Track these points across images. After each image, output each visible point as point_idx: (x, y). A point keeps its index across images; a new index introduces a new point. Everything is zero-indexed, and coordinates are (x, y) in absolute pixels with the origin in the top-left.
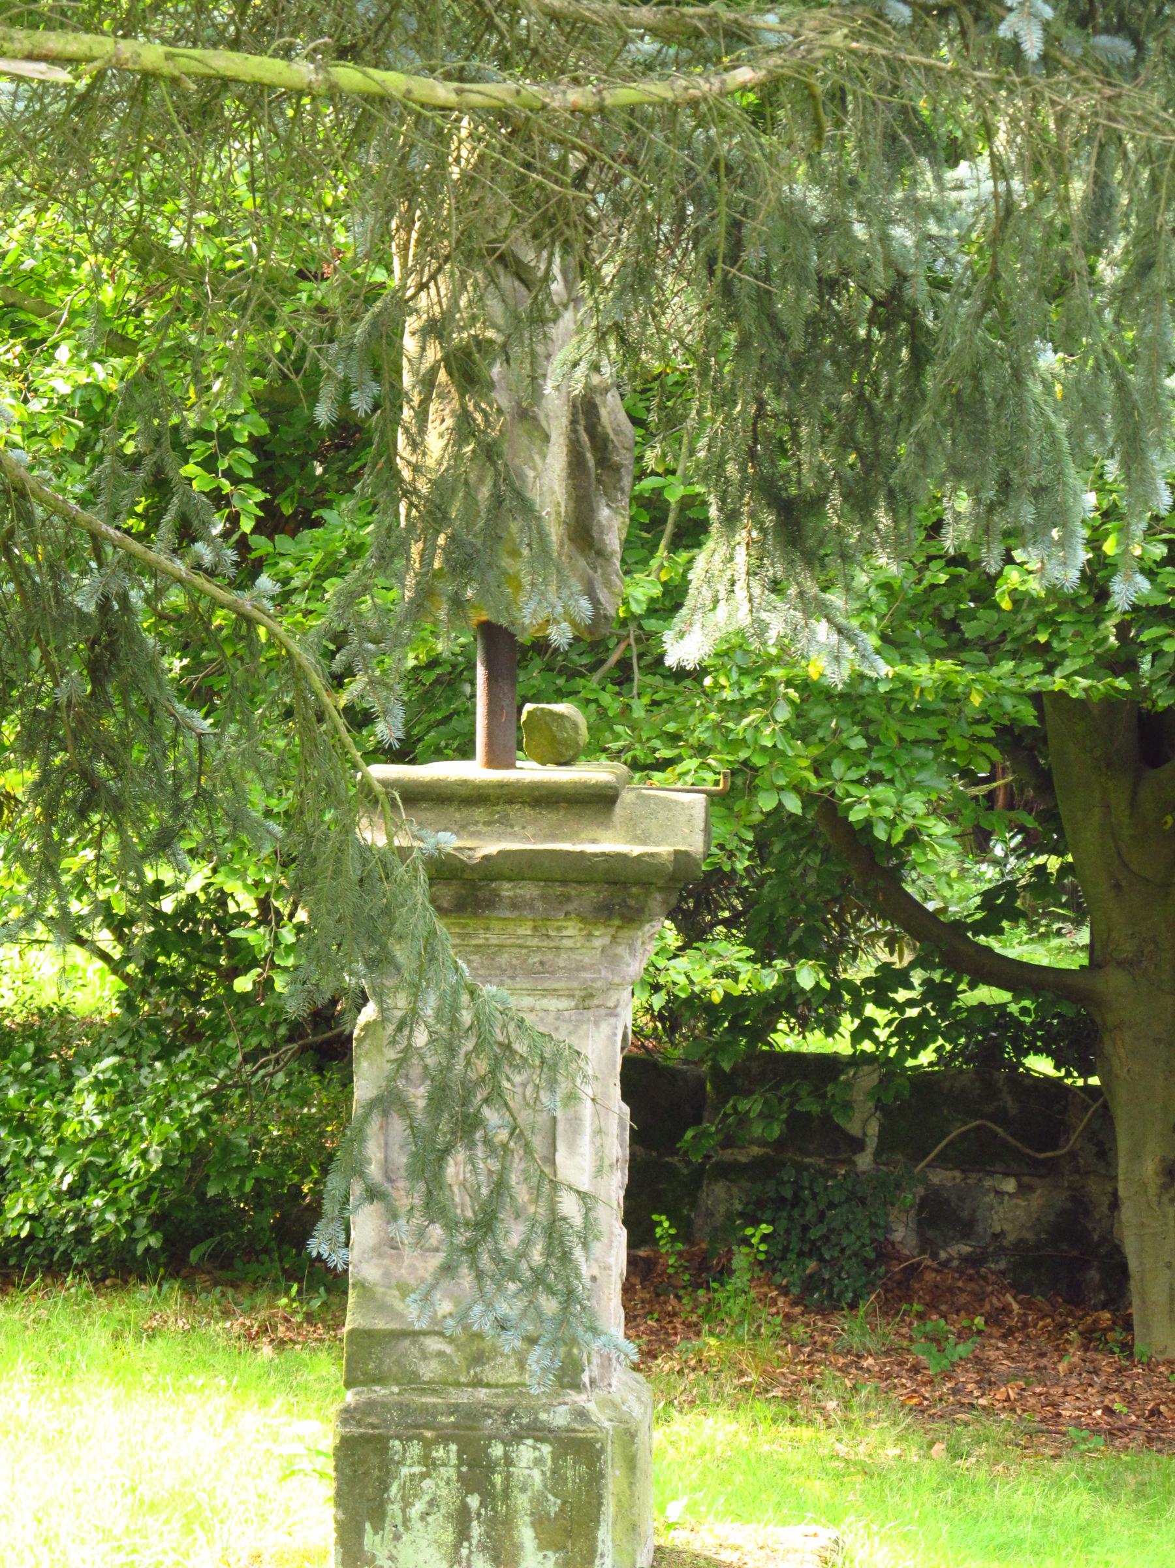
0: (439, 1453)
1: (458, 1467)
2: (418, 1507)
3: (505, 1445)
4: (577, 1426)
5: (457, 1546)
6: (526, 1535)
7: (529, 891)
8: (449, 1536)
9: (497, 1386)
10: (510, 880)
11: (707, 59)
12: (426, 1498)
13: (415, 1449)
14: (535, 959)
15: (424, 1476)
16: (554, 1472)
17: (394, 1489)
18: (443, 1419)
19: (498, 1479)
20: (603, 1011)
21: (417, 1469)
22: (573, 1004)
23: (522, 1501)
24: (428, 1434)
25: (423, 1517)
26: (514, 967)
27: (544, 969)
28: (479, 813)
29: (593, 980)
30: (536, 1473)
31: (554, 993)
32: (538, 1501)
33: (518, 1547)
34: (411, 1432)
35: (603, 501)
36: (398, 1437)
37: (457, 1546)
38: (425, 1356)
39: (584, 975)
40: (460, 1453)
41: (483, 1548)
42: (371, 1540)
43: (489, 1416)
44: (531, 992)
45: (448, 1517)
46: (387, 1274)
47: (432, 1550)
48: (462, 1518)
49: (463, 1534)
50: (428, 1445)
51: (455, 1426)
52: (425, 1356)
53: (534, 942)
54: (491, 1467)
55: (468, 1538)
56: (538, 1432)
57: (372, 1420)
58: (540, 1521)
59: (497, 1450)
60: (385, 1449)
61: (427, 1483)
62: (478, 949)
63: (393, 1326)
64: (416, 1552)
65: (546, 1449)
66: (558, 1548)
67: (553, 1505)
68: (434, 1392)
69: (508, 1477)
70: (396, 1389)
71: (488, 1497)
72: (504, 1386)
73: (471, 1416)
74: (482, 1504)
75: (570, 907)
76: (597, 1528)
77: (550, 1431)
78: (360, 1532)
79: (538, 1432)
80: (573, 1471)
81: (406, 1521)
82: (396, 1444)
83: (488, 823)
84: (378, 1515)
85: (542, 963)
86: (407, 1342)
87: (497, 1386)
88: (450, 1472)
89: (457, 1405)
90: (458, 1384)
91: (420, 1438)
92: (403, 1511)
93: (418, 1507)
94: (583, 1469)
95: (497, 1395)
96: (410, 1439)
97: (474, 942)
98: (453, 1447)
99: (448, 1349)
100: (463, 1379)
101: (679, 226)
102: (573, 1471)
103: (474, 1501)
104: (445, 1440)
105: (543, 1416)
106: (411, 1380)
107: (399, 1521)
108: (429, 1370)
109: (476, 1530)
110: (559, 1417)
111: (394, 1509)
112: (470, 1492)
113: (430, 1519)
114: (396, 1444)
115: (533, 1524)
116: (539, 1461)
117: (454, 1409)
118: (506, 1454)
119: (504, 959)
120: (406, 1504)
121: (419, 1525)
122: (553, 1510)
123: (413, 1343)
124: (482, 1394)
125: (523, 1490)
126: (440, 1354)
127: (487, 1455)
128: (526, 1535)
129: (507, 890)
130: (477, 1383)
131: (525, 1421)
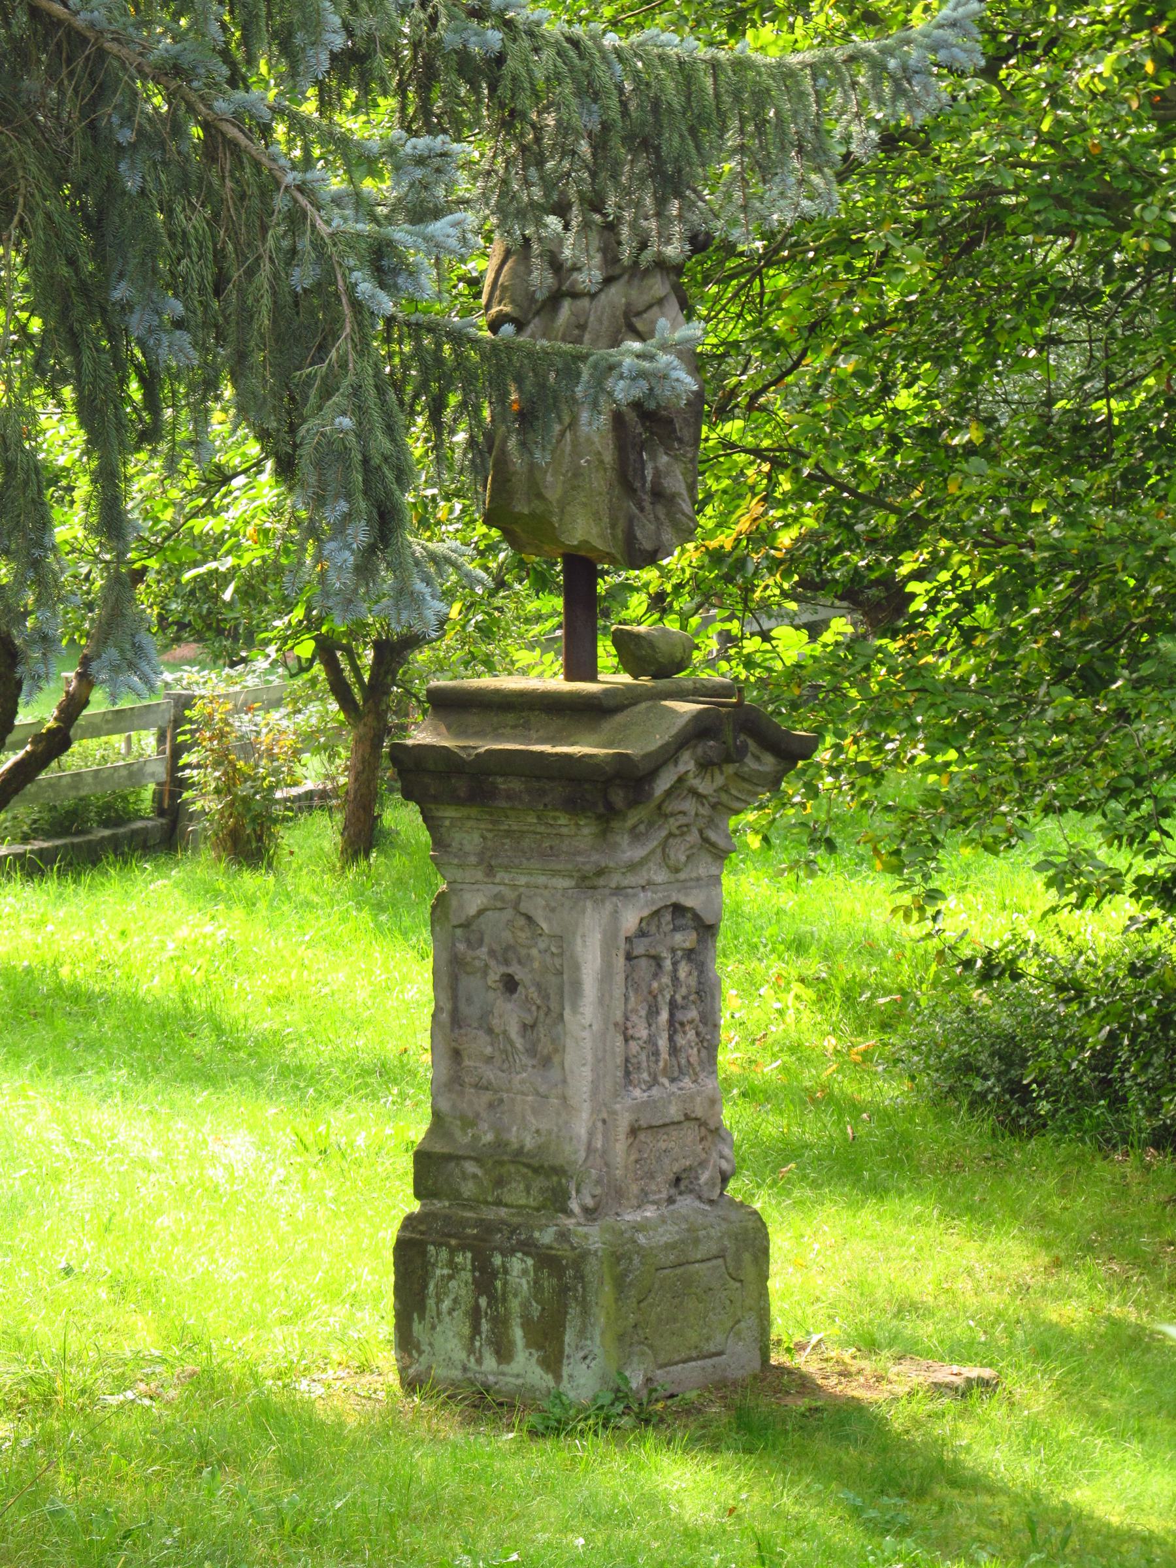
0: (459, 1259)
1: (473, 1270)
2: (446, 1304)
3: (504, 1255)
4: (555, 1245)
5: (472, 1339)
6: (518, 1334)
7: (516, 785)
8: (466, 1331)
9: (512, 1206)
10: (502, 775)
11: (237, 145)
12: (452, 1296)
13: (444, 1254)
14: (546, 844)
15: (451, 1277)
16: (535, 1283)
17: (431, 1287)
18: (469, 1231)
19: (499, 1284)
20: (607, 891)
21: (446, 1272)
22: (573, 883)
23: (515, 1305)
24: (453, 1242)
25: (451, 1311)
26: (532, 850)
27: (552, 853)
28: (510, 718)
29: (584, 864)
30: (524, 1281)
31: (555, 873)
32: (525, 1305)
33: (512, 1343)
34: (442, 1240)
35: (661, 450)
36: (433, 1243)
37: (472, 1339)
38: (464, 1177)
39: (580, 859)
40: (473, 1260)
41: (490, 1343)
42: (417, 1328)
43: (500, 1231)
44: (544, 871)
45: (466, 1313)
46: (454, 1106)
47: (456, 1341)
48: (475, 1315)
49: (476, 1330)
50: (453, 1251)
51: (475, 1237)
52: (464, 1177)
53: (541, 829)
54: (494, 1275)
55: (479, 1333)
56: (528, 1247)
57: (422, 1228)
58: (527, 1324)
59: (497, 1260)
60: (424, 1253)
61: (453, 1284)
62: (509, 833)
63: (446, 1150)
64: (446, 1341)
65: (530, 1262)
66: (540, 1347)
67: (536, 1310)
68: (472, 1208)
69: (505, 1284)
70: (447, 1204)
71: (492, 1299)
72: (517, 1207)
73: (488, 1228)
74: (489, 1305)
75: (547, 800)
76: (564, 1333)
77: (536, 1246)
78: (410, 1320)
79: (528, 1247)
80: (549, 1283)
81: (439, 1314)
82: (431, 1248)
83: (514, 727)
84: (421, 1308)
85: (551, 848)
86: (453, 1164)
87: (512, 1206)
88: (466, 1276)
89: (483, 1220)
90: (486, 1203)
91: (448, 1245)
92: (437, 1304)
93: (446, 1304)
94: (555, 1281)
95: (513, 1215)
96: (441, 1245)
97: (502, 828)
98: (469, 1255)
99: (480, 1172)
100: (490, 1199)
101: (87, 296)
102: (549, 1283)
103: (483, 1302)
104: (463, 1248)
105: (537, 1234)
106: (456, 1195)
107: (434, 1314)
108: (468, 1189)
109: (485, 1326)
110: (546, 1237)
111: (431, 1302)
112: (480, 1294)
113: (455, 1314)
114: (431, 1248)
115: (523, 1325)
116: (525, 1272)
117: (480, 1223)
118: (503, 1265)
119: (526, 843)
120: (439, 1301)
121: (447, 1319)
122: (536, 1314)
123: (457, 1165)
124: (503, 1212)
125: (515, 1295)
126: (475, 1176)
127: (491, 1263)
128: (518, 1334)
129: (502, 784)
130: (499, 1203)
131: (523, 1237)
